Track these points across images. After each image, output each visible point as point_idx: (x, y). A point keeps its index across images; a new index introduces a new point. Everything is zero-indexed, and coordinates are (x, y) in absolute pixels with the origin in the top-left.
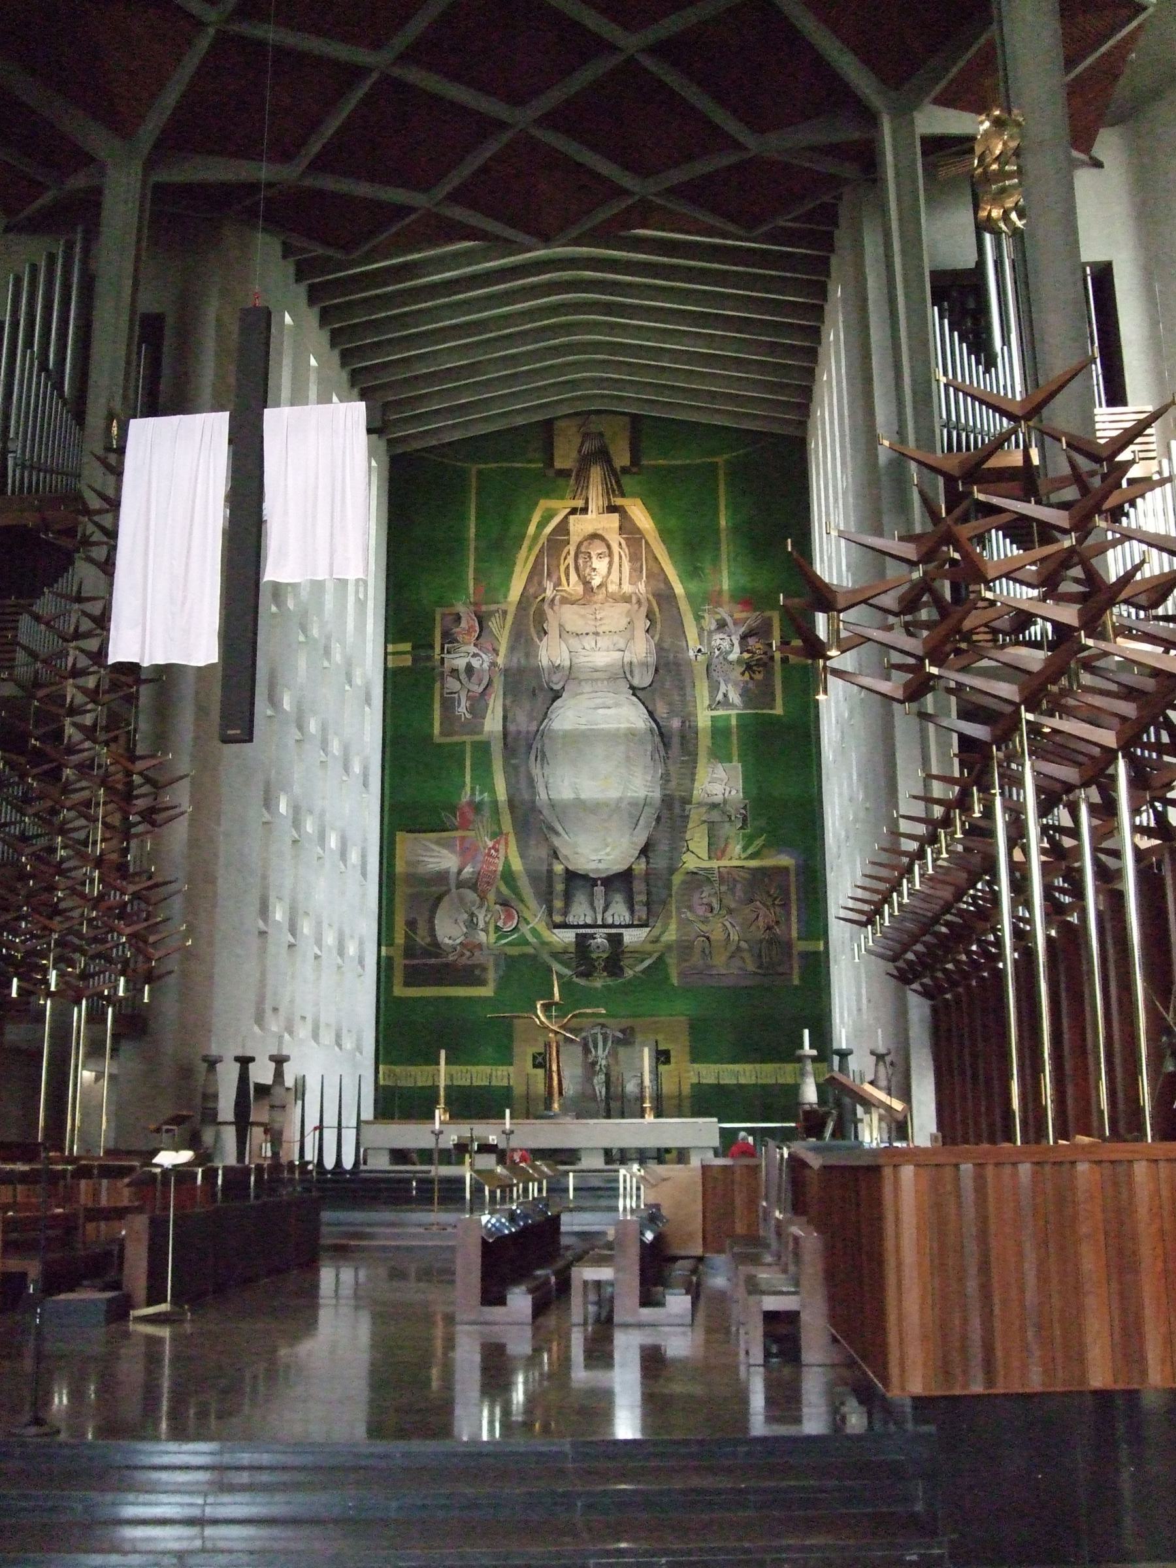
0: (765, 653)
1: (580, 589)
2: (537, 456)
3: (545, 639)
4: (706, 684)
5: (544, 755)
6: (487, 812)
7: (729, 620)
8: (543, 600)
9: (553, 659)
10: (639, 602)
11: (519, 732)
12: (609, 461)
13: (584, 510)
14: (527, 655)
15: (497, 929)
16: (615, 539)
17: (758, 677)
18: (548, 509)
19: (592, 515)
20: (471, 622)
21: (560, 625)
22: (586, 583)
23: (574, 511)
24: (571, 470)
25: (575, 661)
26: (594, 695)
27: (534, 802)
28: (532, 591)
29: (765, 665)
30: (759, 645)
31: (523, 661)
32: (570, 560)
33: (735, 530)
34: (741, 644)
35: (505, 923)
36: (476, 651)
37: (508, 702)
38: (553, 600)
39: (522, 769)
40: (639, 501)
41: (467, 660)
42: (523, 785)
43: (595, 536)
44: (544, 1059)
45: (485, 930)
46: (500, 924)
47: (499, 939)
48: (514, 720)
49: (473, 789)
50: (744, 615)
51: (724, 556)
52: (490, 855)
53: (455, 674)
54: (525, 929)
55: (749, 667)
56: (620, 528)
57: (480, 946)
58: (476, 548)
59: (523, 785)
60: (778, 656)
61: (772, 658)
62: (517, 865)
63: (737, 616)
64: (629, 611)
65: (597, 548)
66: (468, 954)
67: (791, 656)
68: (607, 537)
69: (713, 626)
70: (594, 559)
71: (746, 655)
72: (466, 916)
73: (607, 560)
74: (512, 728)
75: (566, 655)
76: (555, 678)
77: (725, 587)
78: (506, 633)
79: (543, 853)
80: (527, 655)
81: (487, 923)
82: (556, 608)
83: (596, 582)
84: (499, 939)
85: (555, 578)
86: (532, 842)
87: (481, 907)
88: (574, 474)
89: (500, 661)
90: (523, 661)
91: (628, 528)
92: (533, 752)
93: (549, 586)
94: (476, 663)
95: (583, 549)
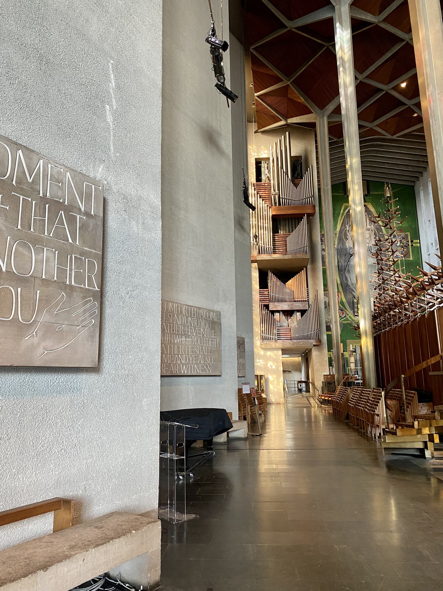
0: (407, 244)
2: (341, 192)
3: (347, 241)
5: (349, 271)
7: (396, 235)
8: (346, 230)
9: (350, 246)
10: (372, 230)
11: (342, 265)
14: (343, 245)
15: (340, 316)
17: (405, 250)
18: (345, 206)
27: (347, 283)
28: (343, 228)
29: (407, 246)
30: (405, 242)
31: (342, 247)
34: (400, 242)
35: (342, 315)
37: (339, 258)
38: (349, 230)
39: (344, 275)
40: (370, 203)
42: (344, 279)
44: (355, 350)
46: (341, 315)
47: (341, 319)
48: (340, 262)
50: (401, 233)
53: (324, 250)
54: (348, 317)
55: (402, 247)
59: (344, 279)
60: (410, 244)
61: (409, 245)
62: (344, 300)
63: (398, 234)
64: (370, 233)
67: (413, 244)
71: (402, 244)
74: (340, 264)
76: (351, 251)
78: (337, 239)
79: (351, 296)
80: (343, 245)
82: (350, 232)
84: (341, 319)
85: (349, 224)
86: (348, 294)
89: (336, 246)
90: (342, 247)
92: (346, 270)
93: (347, 226)
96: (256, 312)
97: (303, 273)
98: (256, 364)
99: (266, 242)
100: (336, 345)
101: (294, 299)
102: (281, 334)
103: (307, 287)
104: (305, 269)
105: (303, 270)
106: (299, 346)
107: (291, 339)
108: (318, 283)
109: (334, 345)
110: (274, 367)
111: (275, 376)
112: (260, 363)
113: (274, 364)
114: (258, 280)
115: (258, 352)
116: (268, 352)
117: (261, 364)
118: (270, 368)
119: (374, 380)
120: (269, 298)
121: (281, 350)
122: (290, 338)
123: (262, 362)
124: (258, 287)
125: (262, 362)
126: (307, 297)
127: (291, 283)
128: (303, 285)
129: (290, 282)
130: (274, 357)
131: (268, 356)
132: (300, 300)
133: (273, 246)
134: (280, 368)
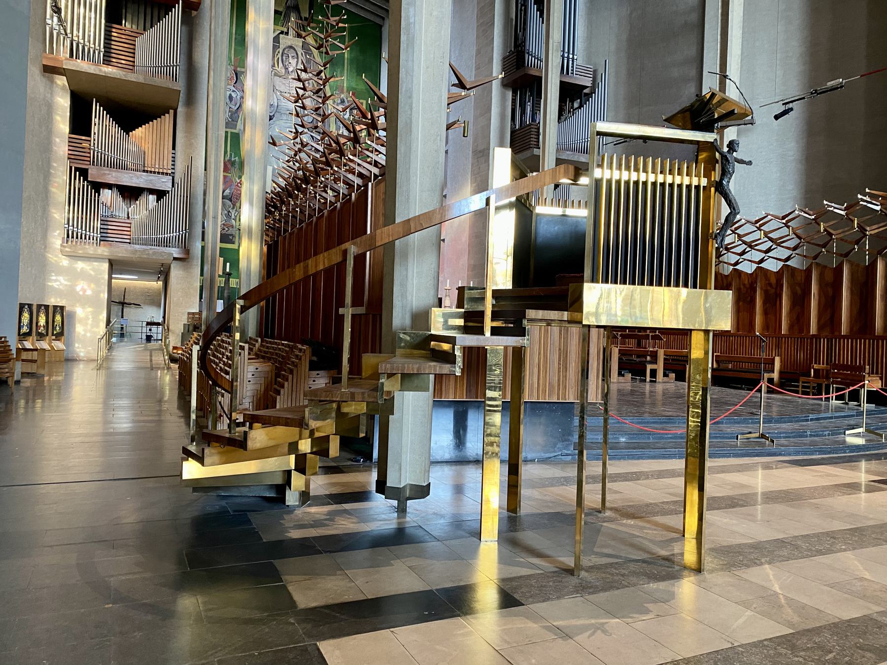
1: (283, 71)
4: (335, 127)
6: (237, 166)
12: (299, 12)
13: (287, 34)
16: (300, 51)
19: (290, 37)
20: (232, 75)
21: (274, 86)
22: (286, 69)
23: (282, 33)
24: (282, 12)
25: (279, 104)
26: (287, 121)
32: (280, 55)
33: (351, 61)
34: (350, 113)
36: (234, 89)
41: (230, 93)
43: (291, 47)
45: (235, 220)
49: (231, 155)
51: (346, 71)
52: (237, 185)
56: (302, 47)
57: (232, 227)
58: (235, 39)
65: (292, 53)
66: (226, 229)
68: (296, 49)
69: (339, 101)
70: (290, 58)
72: (226, 212)
73: (296, 60)
75: (276, 101)
77: (345, 85)
81: (236, 216)
83: (291, 69)
87: (233, 208)
88: (283, 14)
91: (305, 46)
94: (234, 95)
95: (286, 52)
96: (57, 180)
97: (168, 119)
98: (50, 284)
99: (89, 36)
100: (210, 259)
101: (144, 167)
102: (109, 231)
103: (174, 148)
104: (172, 112)
105: (168, 113)
106: (145, 256)
107: (130, 243)
108: (195, 144)
109: (208, 258)
110: (89, 292)
111: (90, 309)
112: (58, 283)
113: (89, 286)
114: (68, 114)
115: (56, 261)
116: (79, 262)
117: (61, 284)
118: (81, 293)
119: (255, 323)
120: (90, 157)
121: (107, 260)
122: (128, 241)
123: (63, 281)
124: (67, 130)
125: (63, 281)
126: (170, 167)
127: (140, 134)
128: (166, 143)
129: (139, 132)
130: (92, 273)
131: (79, 270)
132: (157, 170)
133: (104, 47)
134: (102, 295)
